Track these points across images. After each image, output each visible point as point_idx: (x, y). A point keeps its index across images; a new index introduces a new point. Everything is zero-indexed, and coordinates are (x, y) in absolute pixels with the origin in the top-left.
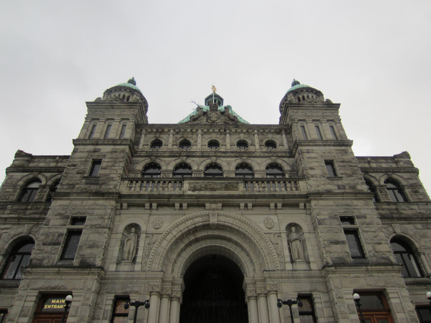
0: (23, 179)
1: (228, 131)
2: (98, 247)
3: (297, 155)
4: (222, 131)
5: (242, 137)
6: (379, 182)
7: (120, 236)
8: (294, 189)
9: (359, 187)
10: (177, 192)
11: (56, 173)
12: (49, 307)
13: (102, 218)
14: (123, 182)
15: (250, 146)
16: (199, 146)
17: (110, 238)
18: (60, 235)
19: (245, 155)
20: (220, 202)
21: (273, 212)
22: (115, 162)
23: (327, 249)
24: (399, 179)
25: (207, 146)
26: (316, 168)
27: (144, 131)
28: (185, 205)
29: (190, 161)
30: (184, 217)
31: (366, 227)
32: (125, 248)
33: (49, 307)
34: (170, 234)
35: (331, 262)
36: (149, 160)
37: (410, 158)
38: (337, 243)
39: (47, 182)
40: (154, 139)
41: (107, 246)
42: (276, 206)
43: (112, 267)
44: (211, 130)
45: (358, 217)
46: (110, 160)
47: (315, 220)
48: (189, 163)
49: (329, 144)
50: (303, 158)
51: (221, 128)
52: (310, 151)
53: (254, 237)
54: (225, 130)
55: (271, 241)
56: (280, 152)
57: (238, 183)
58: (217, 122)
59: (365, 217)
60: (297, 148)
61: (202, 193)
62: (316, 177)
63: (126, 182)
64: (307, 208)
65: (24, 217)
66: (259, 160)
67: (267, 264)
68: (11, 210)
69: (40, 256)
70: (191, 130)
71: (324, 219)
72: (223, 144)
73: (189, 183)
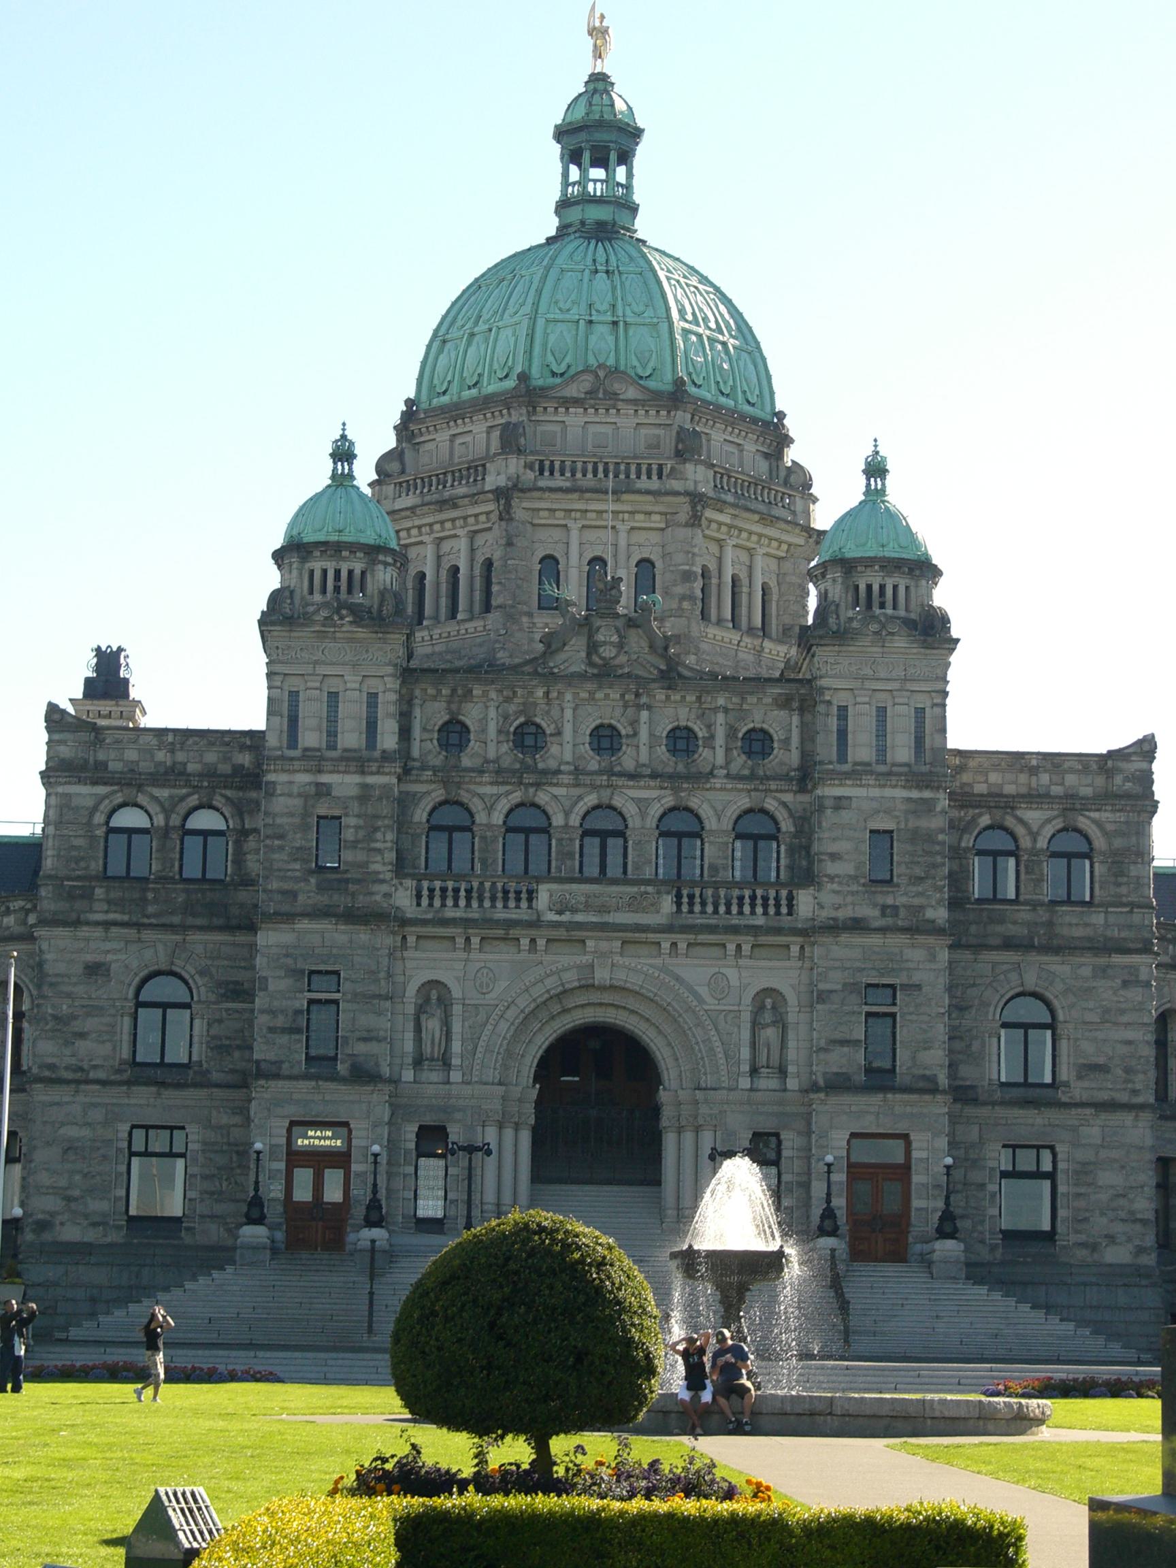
0: (102, 807)
1: (644, 700)
2: (379, 1040)
6: (1035, 841)
7: (411, 1009)
8: (784, 910)
9: (930, 914)
10: (523, 913)
11: (184, 791)
12: (306, 1142)
14: (401, 884)
18: (298, 1012)
19: (685, 786)
20: (617, 939)
21: (731, 961)
22: (376, 829)
23: (822, 1056)
24: (1093, 831)
26: (846, 857)
28: (541, 943)
29: (547, 799)
31: (911, 1014)
32: (424, 1035)
33: (306, 1142)
34: (513, 1007)
35: (821, 1082)
36: (442, 791)
37: (1151, 758)
38: (843, 1042)
39: (167, 818)
40: (446, 718)
42: (739, 947)
43: (408, 1075)
44: (600, 695)
45: (905, 987)
46: (361, 822)
49: (894, 783)
51: (628, 691)
52: (844, 803)
54: (637, 695)
56: (774, 779)
57: (659, 892)
58: (617, 662)
59: (918, 987)
61: (579, 918)
62: (840, 883)
63: (409, 883)
65: (146, 921)
67: (705, 1074)
68: (109, 902)
69: (271, 1056)
70: (547, 694)
71: (831, 991)
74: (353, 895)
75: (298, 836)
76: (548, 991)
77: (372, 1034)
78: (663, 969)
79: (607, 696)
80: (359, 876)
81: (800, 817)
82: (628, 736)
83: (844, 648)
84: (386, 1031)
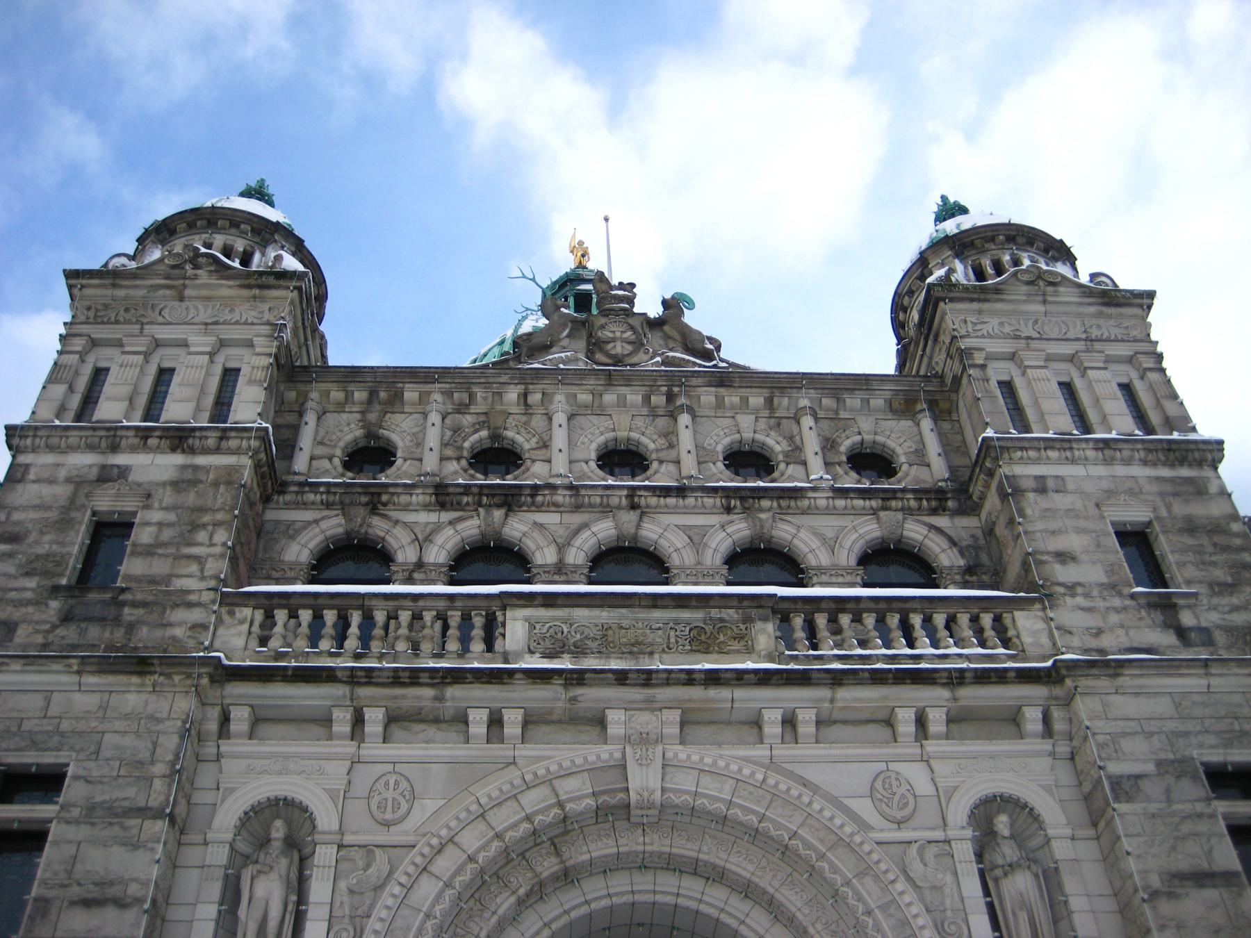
1: (682, 400)
3: (992, 502)
4: (659, 400)
5: (750, 428)
7: (219, 855)
13: (138, 768)
14: (231, 613)
15: (782, 466)
16: (560, 464)
17: (173, 865)
22: (195, 527)
25: (593, 465)
26: (1084, 557)
27: (314, 395)
28: (513, 719)
29: (525, 529)
30: (513, 774)
32: (242, 912)
34: (451, 851)
36: (340, 520)
40: (359, 433)
41: (160, 899)
42: (921, 721)
44: (609, 398)
46: (172, 517)
47: (1099, 780)
48: (517, 535)
50: (1021, 513)
51: (653, 389)
52: (1051, 484)
53: (831, 863)
55: (909, 879)
57: (747, 620)
58: (634, 360)
60: (991, 473)
62: (1087, 596)
63: (247, 612)
64: (1059, 726)
66: (827, 525)
70: (525, 395)
71: (1138, 777)
72: (662, 455)
73: (526, 620)
74: (131, 627)
75: (47, 538)
76: (528, 818)
77: (115, 891)
78: (771, 764)
79: (622, 402)
80: (150, 598)
81: (968, 547)
82: (657, 450)
83: (986, 306)
84: (145, 884)
